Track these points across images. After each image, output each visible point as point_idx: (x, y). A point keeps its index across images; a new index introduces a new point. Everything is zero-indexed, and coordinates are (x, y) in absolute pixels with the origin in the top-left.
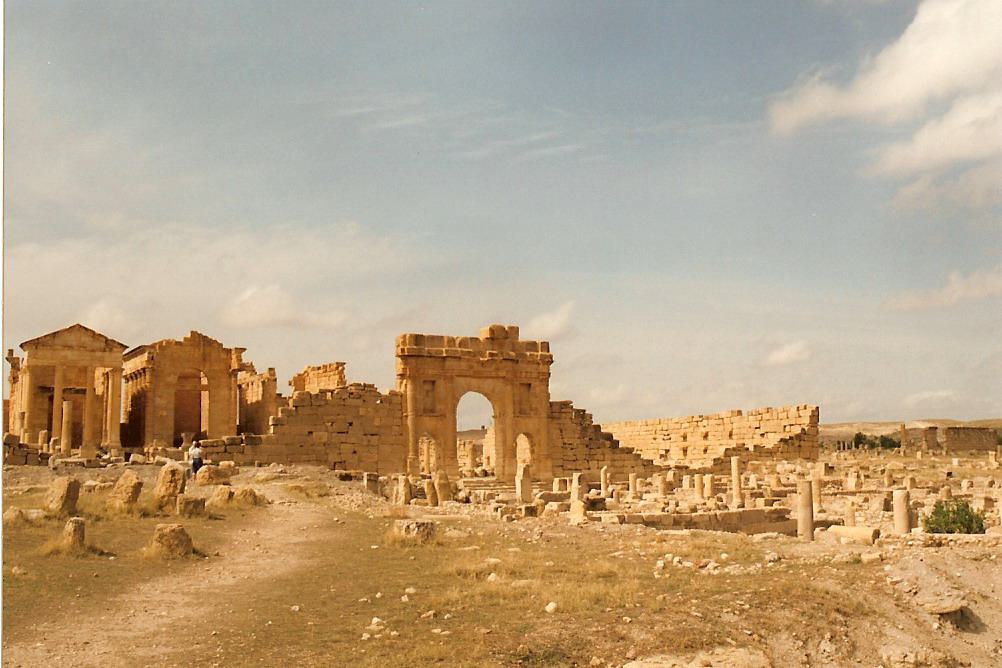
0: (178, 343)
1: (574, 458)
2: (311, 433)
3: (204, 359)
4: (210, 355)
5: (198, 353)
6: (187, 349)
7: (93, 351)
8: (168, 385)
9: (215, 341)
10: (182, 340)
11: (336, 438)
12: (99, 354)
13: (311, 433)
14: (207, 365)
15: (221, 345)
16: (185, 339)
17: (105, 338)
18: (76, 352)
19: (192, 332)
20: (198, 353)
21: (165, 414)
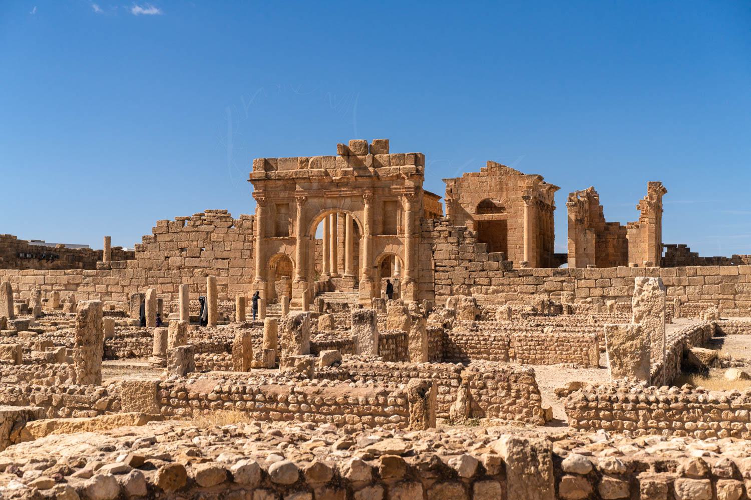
1: (449, 281)
2: (167, 258)
3: (501, 189)
4: (507, 185)
6: (483, 179)
11: (189, 262)
13: (167, 258)
19: (490, 163)
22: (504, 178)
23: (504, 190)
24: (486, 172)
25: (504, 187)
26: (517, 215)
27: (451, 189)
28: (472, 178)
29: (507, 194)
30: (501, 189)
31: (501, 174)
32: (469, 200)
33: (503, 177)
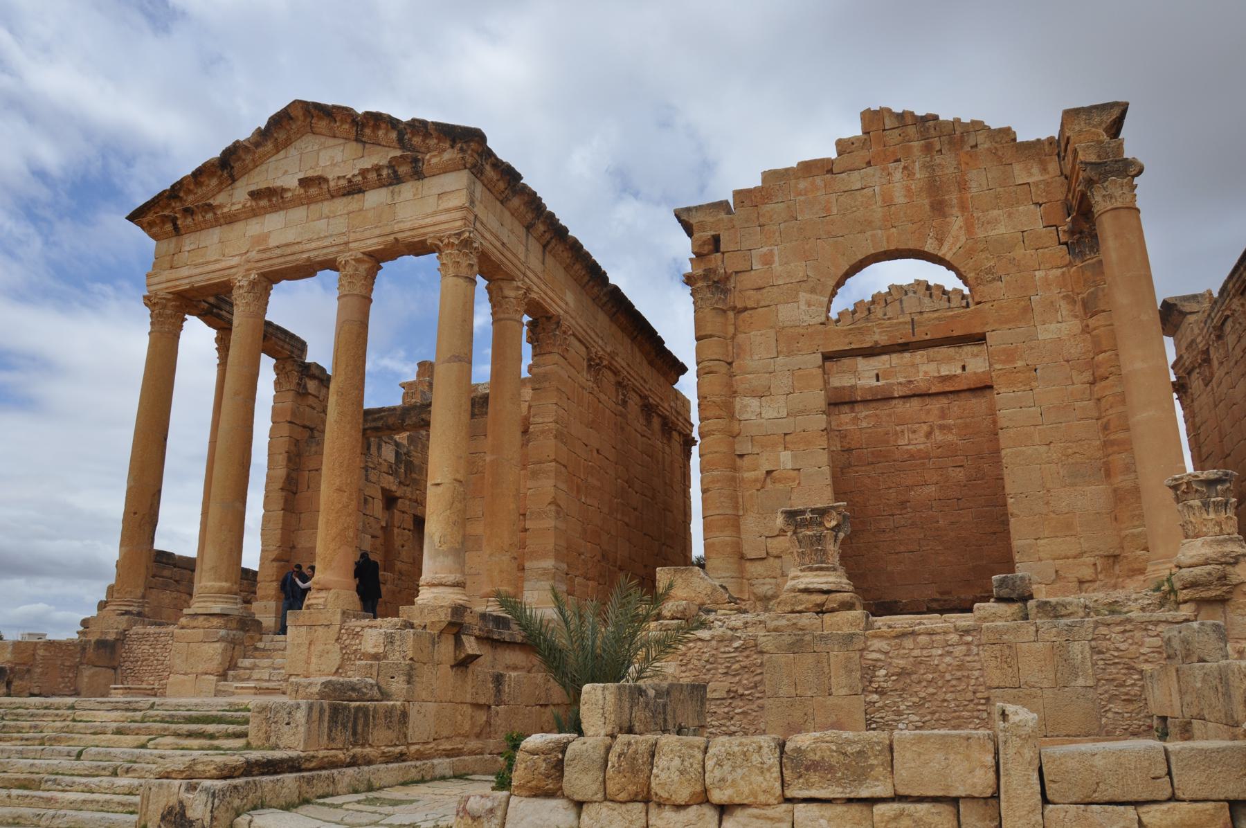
0: (808, 168)
3: (939, 208)
4: (962, 186)
5: (899, 185)
6: (855, 179)
7: (353, 189)
8: (788, 340)
9: (977, 126)
10: (832, 154)
12: (375, 198)
14: (956, 223)
15: (1007, 132)
16: (839, 143)
17: (393, 123)
18: (299, 213)
19: (873, 119)
20: (899, 185)
21: (786, 459)
22: (947, 163)
23: (955, 211)
24: (863, 153)
25: (953, 197)
26: (1027, 310)
27: (716, 240)
28: (802, 185)
29: (969, 228)
30: (939, 208)
31: (928, 149)
32: (799, 269)
33: (938, 159)
